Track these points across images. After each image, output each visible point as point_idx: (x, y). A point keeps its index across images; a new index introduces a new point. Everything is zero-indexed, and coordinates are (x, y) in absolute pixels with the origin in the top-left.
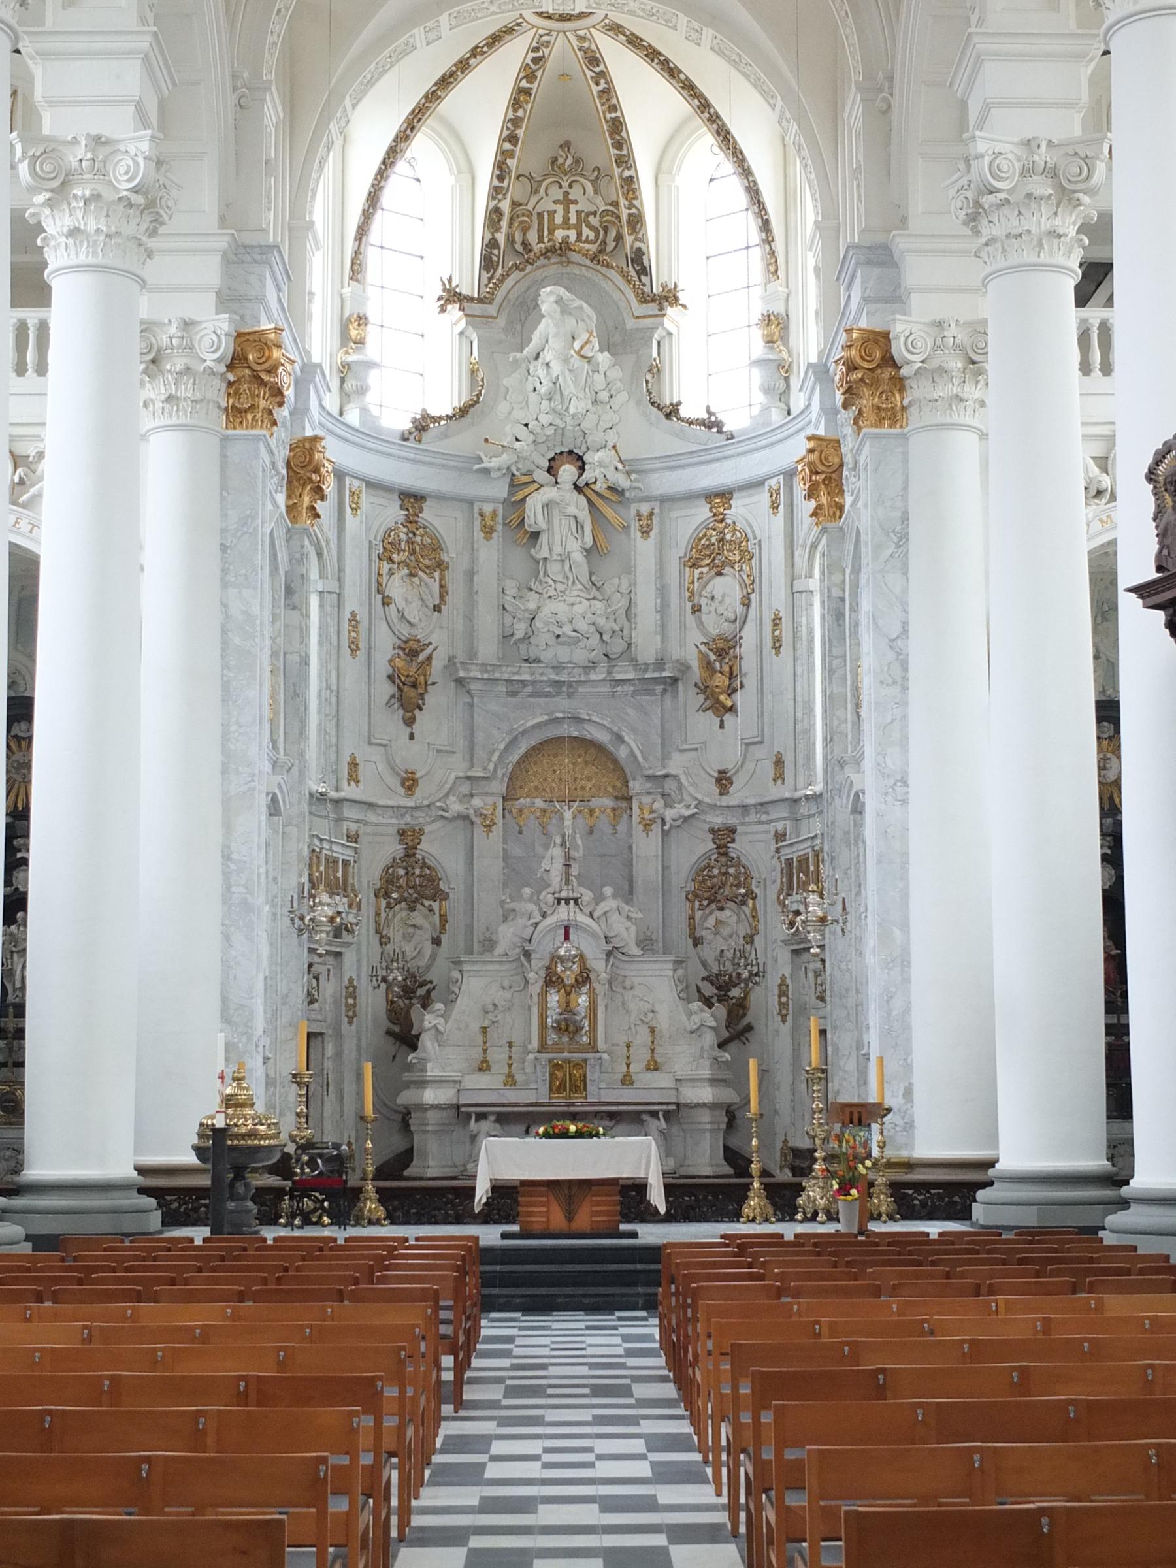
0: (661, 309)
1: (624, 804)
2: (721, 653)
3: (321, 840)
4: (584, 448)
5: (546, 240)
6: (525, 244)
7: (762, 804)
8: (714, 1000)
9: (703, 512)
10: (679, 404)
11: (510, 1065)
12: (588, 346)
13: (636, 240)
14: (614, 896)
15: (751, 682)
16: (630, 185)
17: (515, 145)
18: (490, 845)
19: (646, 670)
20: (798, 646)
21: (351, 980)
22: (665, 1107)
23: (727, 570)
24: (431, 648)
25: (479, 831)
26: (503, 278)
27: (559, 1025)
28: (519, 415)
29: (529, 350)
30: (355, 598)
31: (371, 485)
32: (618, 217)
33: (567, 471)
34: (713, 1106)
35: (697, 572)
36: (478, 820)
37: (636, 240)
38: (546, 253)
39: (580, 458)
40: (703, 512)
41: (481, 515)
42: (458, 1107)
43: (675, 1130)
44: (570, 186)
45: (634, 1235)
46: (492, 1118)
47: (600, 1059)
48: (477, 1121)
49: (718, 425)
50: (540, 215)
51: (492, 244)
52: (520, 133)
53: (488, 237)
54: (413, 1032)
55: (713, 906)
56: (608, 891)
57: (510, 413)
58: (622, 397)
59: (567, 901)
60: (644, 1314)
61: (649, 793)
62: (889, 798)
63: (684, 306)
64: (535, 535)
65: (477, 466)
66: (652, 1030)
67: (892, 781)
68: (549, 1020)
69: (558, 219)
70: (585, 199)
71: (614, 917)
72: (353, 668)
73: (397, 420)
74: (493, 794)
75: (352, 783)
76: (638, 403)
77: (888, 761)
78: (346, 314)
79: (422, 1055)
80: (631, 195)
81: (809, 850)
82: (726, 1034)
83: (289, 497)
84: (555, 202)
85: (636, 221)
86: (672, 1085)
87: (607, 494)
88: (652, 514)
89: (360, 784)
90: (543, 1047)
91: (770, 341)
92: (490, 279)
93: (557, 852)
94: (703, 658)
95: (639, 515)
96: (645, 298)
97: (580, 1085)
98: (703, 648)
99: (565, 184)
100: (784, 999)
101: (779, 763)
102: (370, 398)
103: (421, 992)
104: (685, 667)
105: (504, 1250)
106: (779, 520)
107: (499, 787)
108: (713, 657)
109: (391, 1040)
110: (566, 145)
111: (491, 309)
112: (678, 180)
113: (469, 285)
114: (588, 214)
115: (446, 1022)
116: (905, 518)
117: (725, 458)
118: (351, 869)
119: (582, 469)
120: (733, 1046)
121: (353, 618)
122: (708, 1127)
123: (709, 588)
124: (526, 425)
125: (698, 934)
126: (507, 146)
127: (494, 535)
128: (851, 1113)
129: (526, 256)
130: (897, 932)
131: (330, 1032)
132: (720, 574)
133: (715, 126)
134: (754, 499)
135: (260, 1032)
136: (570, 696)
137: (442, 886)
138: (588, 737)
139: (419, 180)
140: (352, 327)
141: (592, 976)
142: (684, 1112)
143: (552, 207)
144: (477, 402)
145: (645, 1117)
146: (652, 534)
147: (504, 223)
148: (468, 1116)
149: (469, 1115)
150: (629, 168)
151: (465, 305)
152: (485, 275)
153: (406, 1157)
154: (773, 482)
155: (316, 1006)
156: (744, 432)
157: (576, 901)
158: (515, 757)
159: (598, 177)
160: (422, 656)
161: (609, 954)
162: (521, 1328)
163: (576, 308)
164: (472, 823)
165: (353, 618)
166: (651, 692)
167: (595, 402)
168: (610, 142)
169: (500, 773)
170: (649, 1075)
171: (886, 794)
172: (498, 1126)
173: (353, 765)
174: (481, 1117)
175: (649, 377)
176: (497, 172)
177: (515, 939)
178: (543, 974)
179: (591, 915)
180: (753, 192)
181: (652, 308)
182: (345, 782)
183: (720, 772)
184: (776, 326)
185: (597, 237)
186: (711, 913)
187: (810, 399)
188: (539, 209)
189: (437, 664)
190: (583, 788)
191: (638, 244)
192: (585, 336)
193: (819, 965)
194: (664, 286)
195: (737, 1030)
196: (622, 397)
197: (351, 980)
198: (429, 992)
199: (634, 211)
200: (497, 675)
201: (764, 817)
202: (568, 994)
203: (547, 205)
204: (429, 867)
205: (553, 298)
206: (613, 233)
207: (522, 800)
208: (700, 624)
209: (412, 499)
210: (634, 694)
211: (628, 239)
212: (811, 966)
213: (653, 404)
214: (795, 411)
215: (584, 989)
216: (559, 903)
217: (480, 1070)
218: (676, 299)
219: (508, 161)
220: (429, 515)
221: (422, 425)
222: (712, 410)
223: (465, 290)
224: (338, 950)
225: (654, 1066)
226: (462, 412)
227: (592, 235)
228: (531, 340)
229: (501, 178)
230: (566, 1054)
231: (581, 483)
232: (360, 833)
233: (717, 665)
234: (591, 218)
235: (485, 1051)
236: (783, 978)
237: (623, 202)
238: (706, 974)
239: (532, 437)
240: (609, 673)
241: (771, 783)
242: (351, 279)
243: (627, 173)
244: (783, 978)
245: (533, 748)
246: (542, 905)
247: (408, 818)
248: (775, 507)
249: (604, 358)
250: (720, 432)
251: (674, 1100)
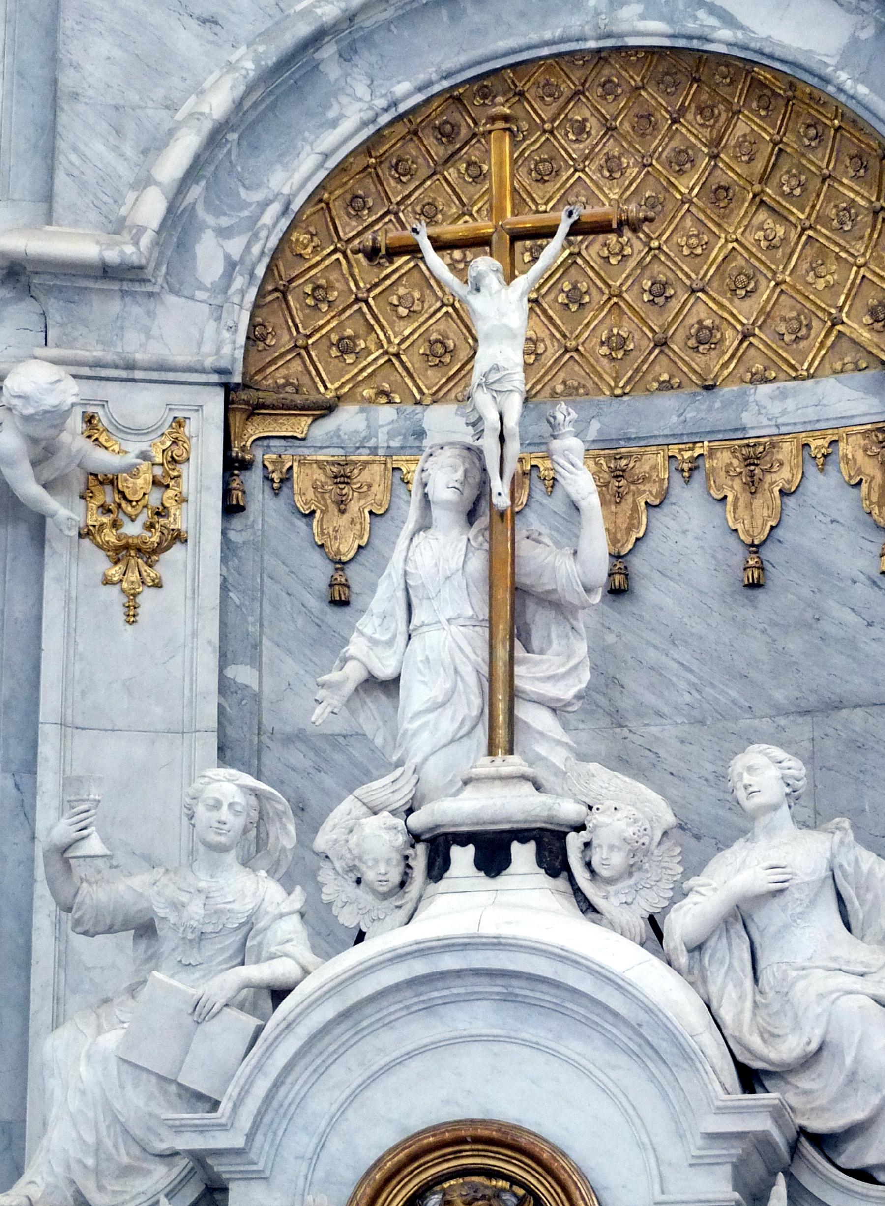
14: (811, 808)
25: (75, 577)
36: (65, 512)
56: (764, 771)
59: (493, 853)
71: (808, 940)
74: (162, 373)
93: (438, 559)
107: (200, 328)
138: (722, 38)
157: (552, 848)
158: (295, 172)
164: (38, 525)
169: (209, 256)
177: (137, 1102)
190: (705, 338)
207: (348, 419)
216: (438, 866)
245: (410, 123)
246: (334, 887)
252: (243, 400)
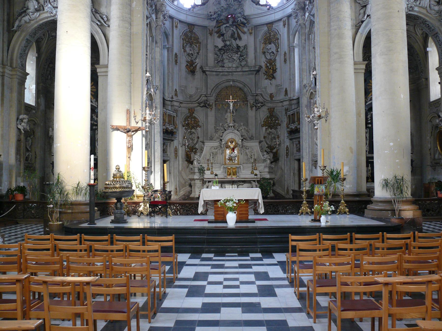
2: (271, 64)
9: (265, 28)
15: (278, 71)
18: (212, 114)
20: (291, 60)
24: (196, 63)
30: (176, 49)
31: (180, 21)
40: (265, 28)
72: (176, 69)
82: (272, 160)
98: (266, 62)
101: (286, 91)
104: (261, 67)
106: (286, 29)
108: (268, 65)
109: (186, 162)
115: (200, 157)
118: (175, 119)
120: (273, 163)
121: (176, 54)
132: (270, 44)
134: (279, 24)
136: (232, 75)
145: (252, 182)
149: (206, 181)
153: (190, 192)
154: (284, 19)
160: (194, 65)
161: (242, 140)
165: (176, 54)
166: (252, 74)
169: (214, 95)
174: (209, 182)
178: (225, 145)
179: (238, 130)
183: (271, 94)
189: (198, 67)
193: (297, 142)
195: (275, 159)
200: (213, 70)
209: (191, 26)
210: (249, 74)
233: (269, 67)
236: (287, 146)
238: (267, 146)
240: (242, 69)
244: (287, 146)
248: (284, 25)
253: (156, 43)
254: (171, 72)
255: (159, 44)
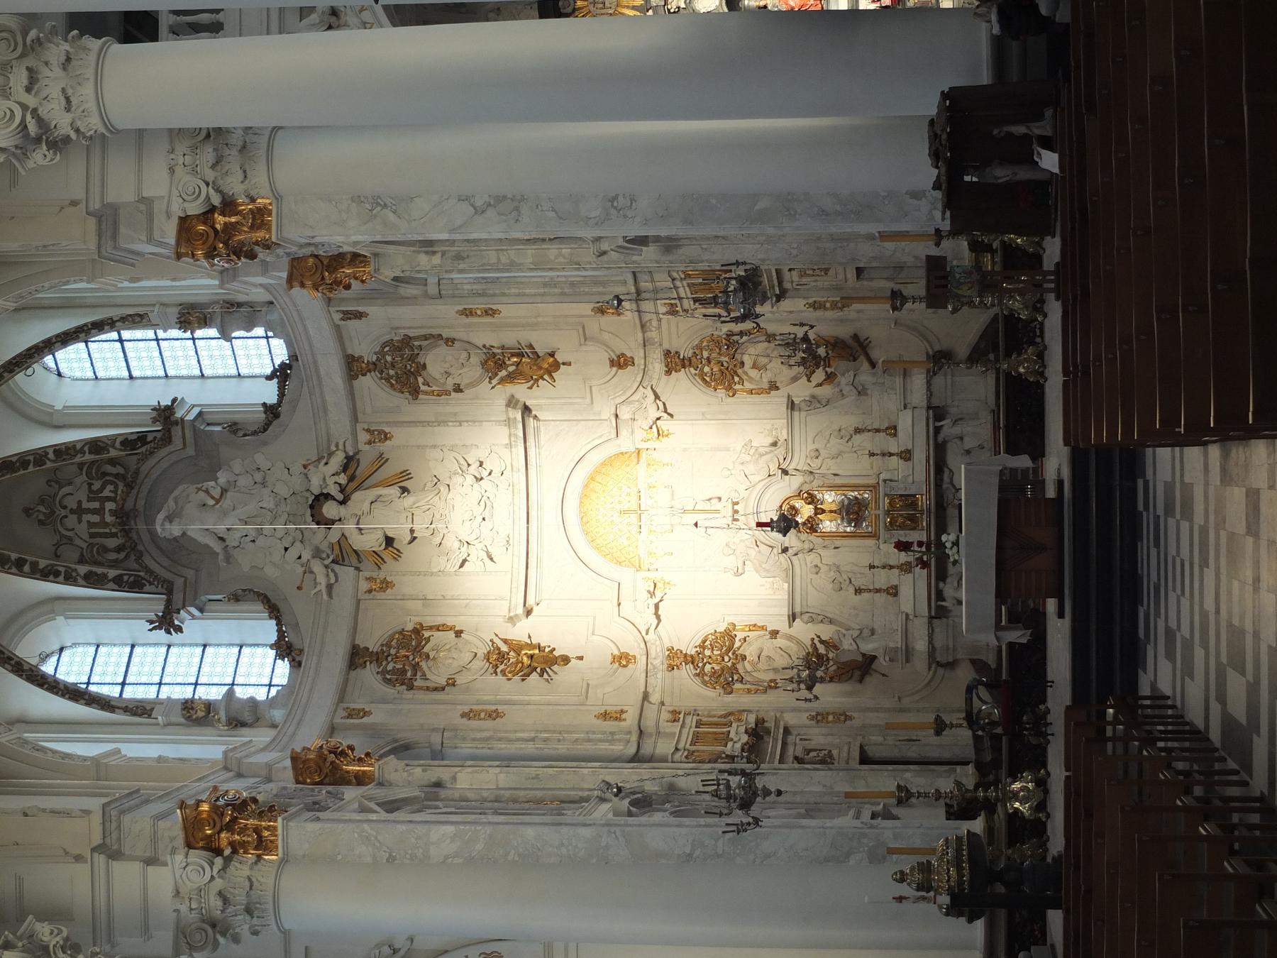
0: (176, 423)
1: (643, 454)
2: (501, 365)
3: (677, 749)
4: (308, 495)
5: (114, 530)
6: (119, 549)
7: (643, 326)
8: (829, 370)
10: (264, 405)
11: (891, 567)
12: (212, 492)
13: (113, 446)
16: (63, 452)
17: (26, 561)
19: (516, 436)
21: (812, 718)
22: (931, 421)
23: (421, 360)
26: (150, 572)
27: (852, 520)
28: (277, 555)
29: (217, 547)
31: (342, 697)
32: (93, 463)
33: (330, 509)
34: (931, 374)
35: (423, 388)
37: (113, 446)
38: (126, 533)
39: (317, 498)
41: (370, 591)
42: (931, 618)
43: (953, 410)
44: (65, 507)
45: (1060, 483)
46: (941, 585)
47: (885, 481)
48: (944, 600)
49: (283, 365)
50: (92, 536)
51: (119, 583)
52: (14, 556)
53: (111, 585)
54: (860, 659)
55: (740, 371)
57: (274, 564)
58: (260, 459)
59: (736, 512)
60: (1140, 482)
61: (633, 432)
62: (629, 214)
63: (174, 400)
64: (389, 541)
65: (325, 597)
66: (858, 431)
67: (613, 211)
68: (848, 529)
69: (95, 518)
70: (77, 494)
73: (283, 667)
75: (624, 716)
76: (265, 443)
77: (593, 214)
78: (183, 720)
79: (881, 651)
80: (72, 452)
81: (685, 283)
83: (349, 783)
84: (80, 521)
85: (96, 446)
86: (909, 413)
87: (350, 472)
88: (368, 431)
89: (625, 708)
90: (874, 535)
91: (205, 322)
92: (151, 584)
94: (502, 381)
95: (369, 443)
96: (166, 439)
97: (909, 501)
98: (494, 382)
99: (63, 512)
100: (828, 305)
102: (261, 695)
103: (822, 650)
105: (1074, 620)
108: (503, 373)
109: (868, 679)
110: (27, 511)
111: (179, 582)
112: (59, 406)
113: (156, 604)
114: (90, 491)
116: (358, 199)
117: (315, 362)
119: (327, 497)
122: (949, 377)
123: (437, 376)
124: (286, 549)
125: (766, 386)
126: (27, 568)
127: (389, 579)
128: (937, 287)
129: (131, 548)
130: (760, 205)
131: (860, 738)
132: (424, 366)
133: (5, 374)
135: (857, 823)
137: (721, 629)
139: (61, 650)
140: (195, 714)
141: (805, 488)
142: (935, 402)
143: (84, 525)
144: (266, 596)
145: (940, 439)
146: (387, 430)
147: (99, 570)
148: (939, 608)
149: (939, 608)
150: (47, 454)
151: (175, 607)
152: (147, 588)
154: (337, 317)
155: (835, 752)
156: (289, 345)
159: (55, 480)
160: (504, 648)
162: (1157, 614)
163: (176, 503)
167: (264, 484)
168: (22, 472)
170: (900, 434)
171: (625, 216)
172: (949, 580)
173: (605, 716)
174: (940, 596)
175: (241, 434)
176: (51, 577)
178: (804, 536)
180: (66, 338)
181: (176, 432)
182: (622, 723)
184: (191, 317)
185: (111, 483)
186: (746, 373)
187: (254, 285)
188: (86, 537)
191: (118, 444)
192: (201, 494)
194: (155, 420)
196: (260, 459)
197: (812, 718)
198: (822, 642)
199: (86, 449)
201: (655, 323)
202: (823, 511)
203: (82, 529)
204: (704, 642)
205: (168, 526)
206: (109, 468)
208: (472, 385)
209: (357, 657)
211: (113, 453)
212: (796, 279)
213: (265, 430)
214: (268, 297)
215: (819, 496)
217: (896, 595)
218: (167, 407)
219: (41, 567)
220: (372, 641)
221: (284, 649)
222: (269, 371)
223: (160, 608)
224: (781, 731)
225: (892, 430)
226: (274, 611)
227: (110, 487)
228: (207, 546)
229: (57, 574)
230: (881, 512)
231: (340, 497)
232: (671, 709)
233: (511, 369)
234: (95, 488)
235: (878, 591)
237: (78, 459)
239: (298, 544)
241: (622, 317)
242: (150, 716)
243: (51, 456)
247: (657, 662)
248: (359, 315)
249: (223, 477)
250: (289, 366)
251: (924, 411)
252: (639, 569)
253: (438, 785)
254: (533, 735)
255: (442, 773)
